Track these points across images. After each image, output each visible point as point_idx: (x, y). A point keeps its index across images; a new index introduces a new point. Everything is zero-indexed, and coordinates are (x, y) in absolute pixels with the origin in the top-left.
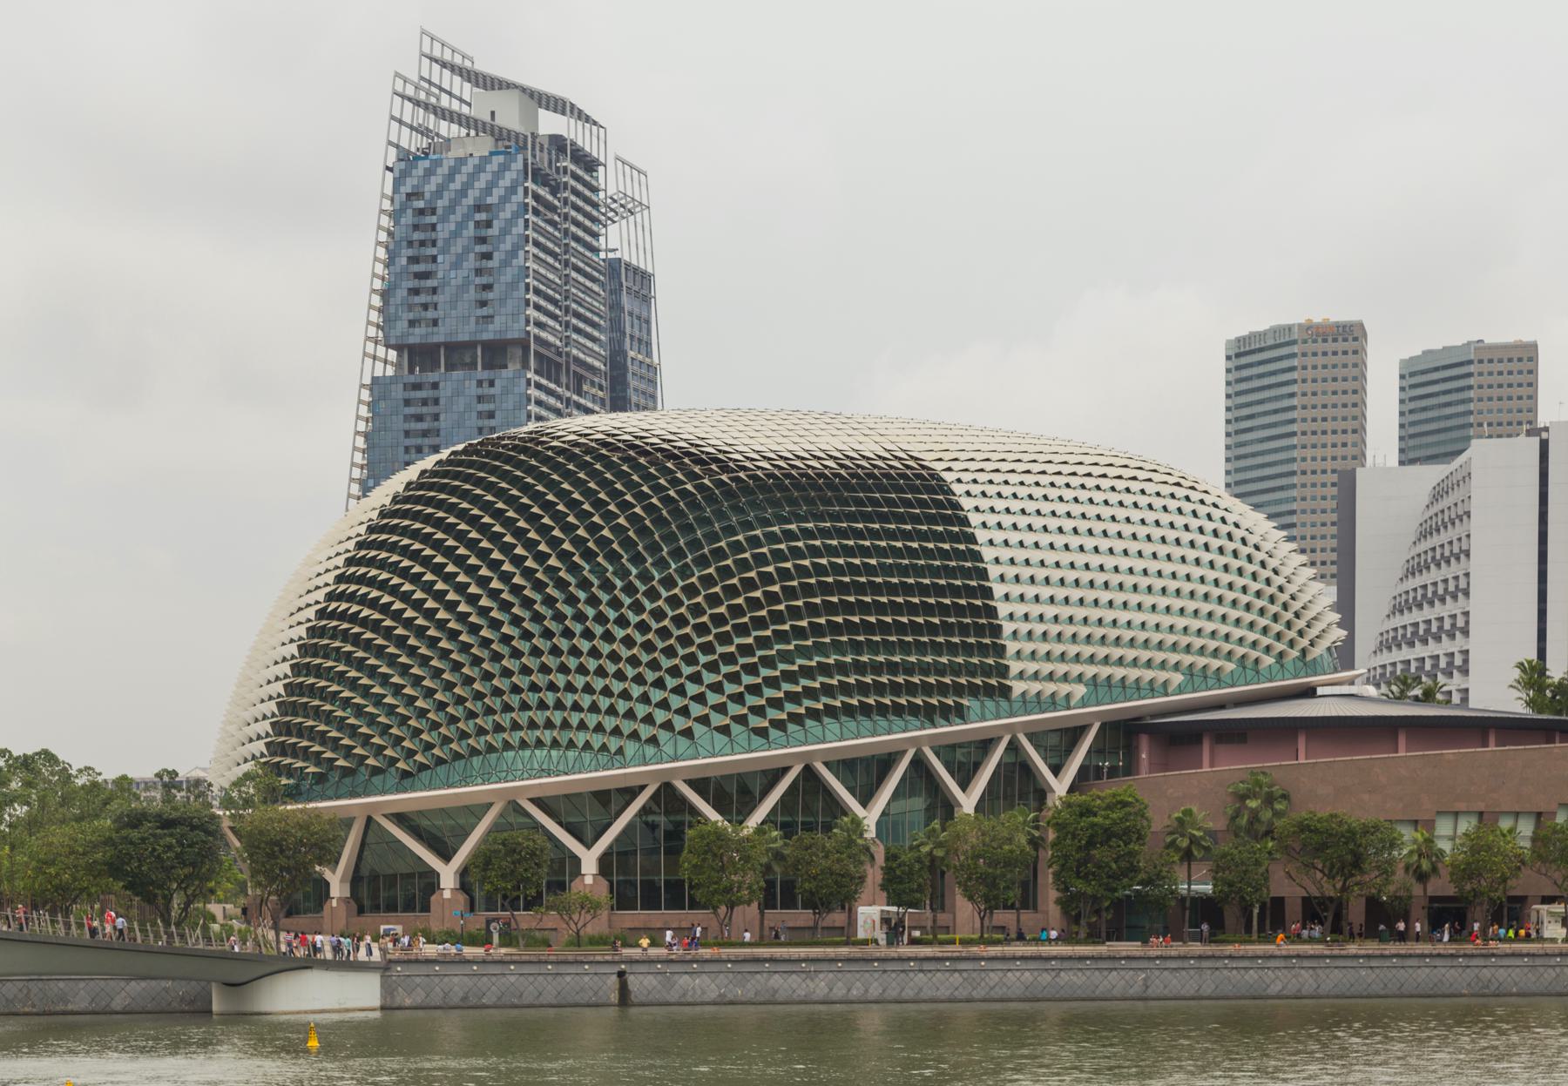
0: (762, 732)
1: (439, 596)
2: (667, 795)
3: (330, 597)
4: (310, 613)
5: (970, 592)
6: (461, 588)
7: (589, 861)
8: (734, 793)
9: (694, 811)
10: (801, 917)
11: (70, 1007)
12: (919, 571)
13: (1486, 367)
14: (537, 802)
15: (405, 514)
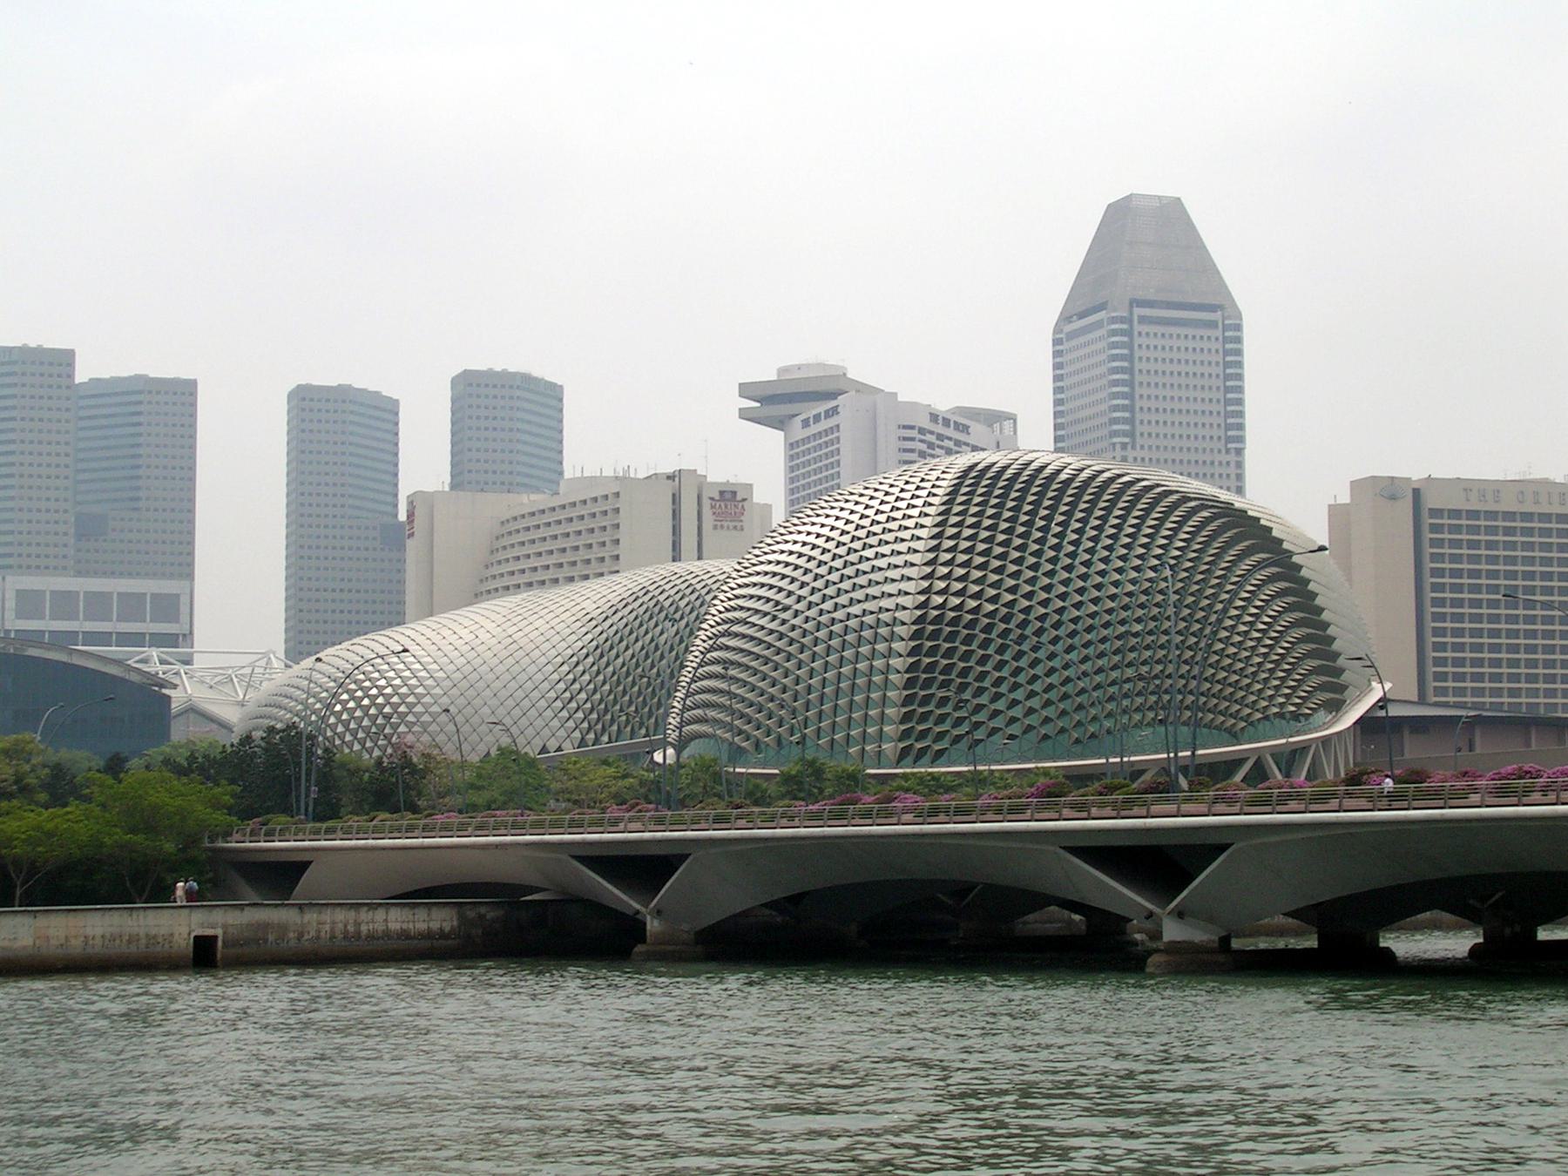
0: (1296, 717)
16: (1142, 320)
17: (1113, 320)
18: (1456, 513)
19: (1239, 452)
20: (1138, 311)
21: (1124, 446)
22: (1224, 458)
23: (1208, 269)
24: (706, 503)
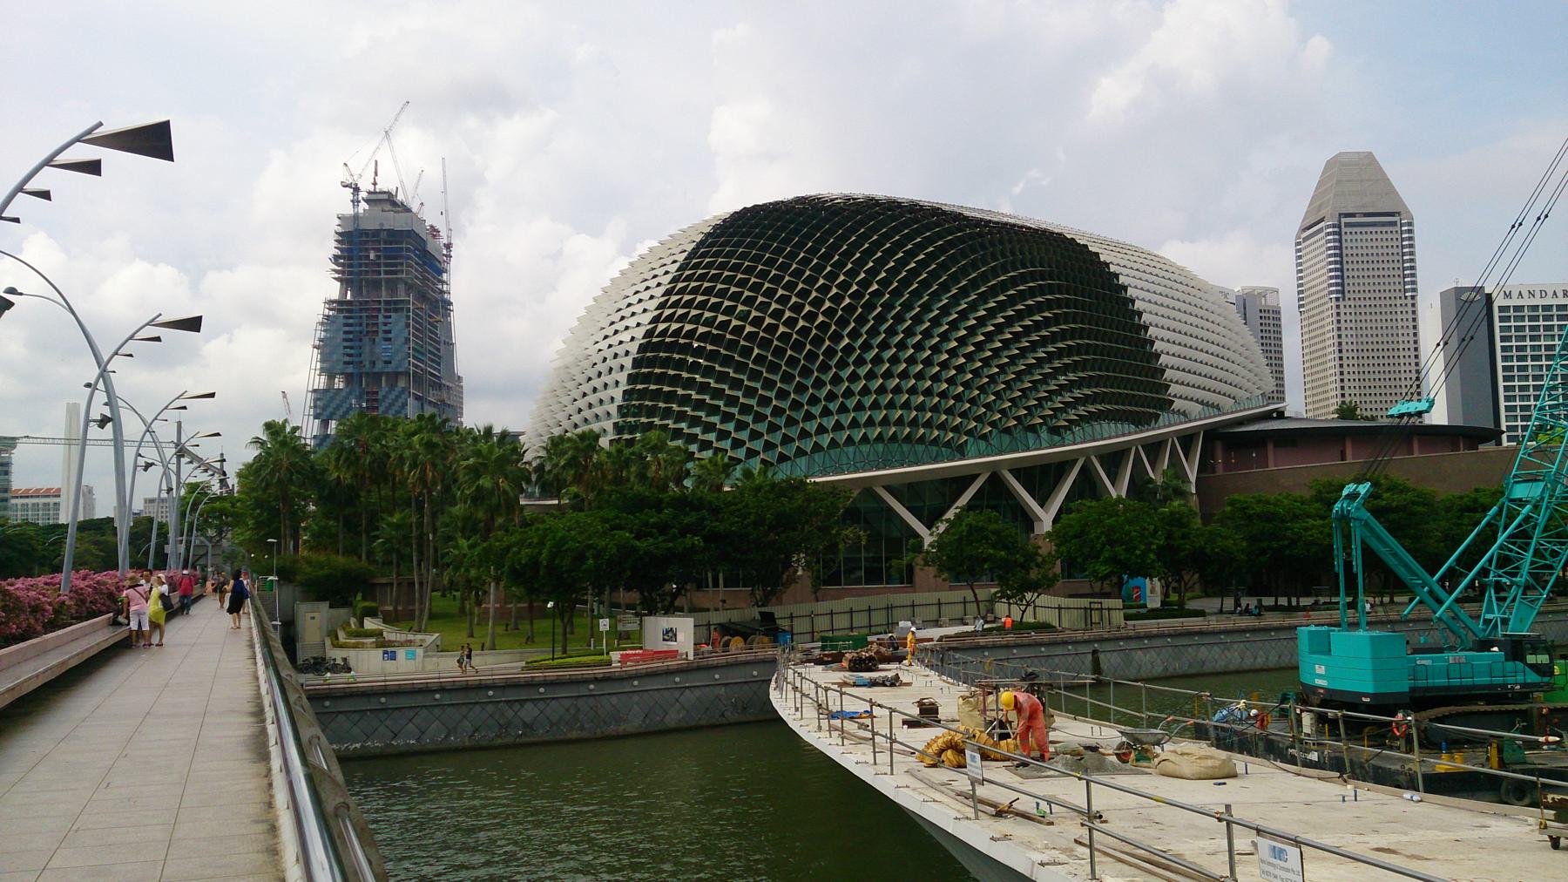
9: (1011, 494)
11: (623, 728)
14: (888, 489)
16: (1347, 225)
19: (1413, 297)
20: (1344, 220)
23: (1391, 191)
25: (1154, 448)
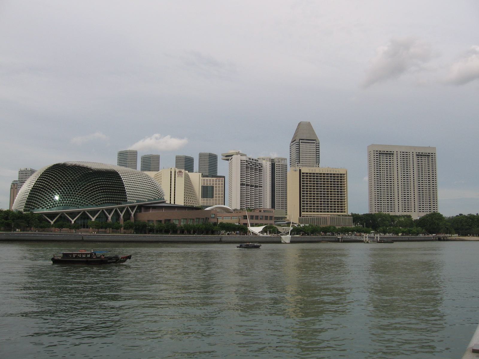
1: (47, 185)
2: (84, 213)
3: (35, 184)
4: (32, 186)
5: (122, 188)
6: (56, 184)
7: (73, 222)
8: (93, 213)
9: (87, 215)
10: (103, 230)
12: (116, 185)
13: (153, 158)
14: (66, 213)
15: (45, 173)
16: (301, 142)
17: (296, 142)
18: (307, 173)
19: (318, 164)
20: (300, 141)
21: (298, 163)
22: (316, 165)
23: (314, 134)
24: (176, 173)
25: (122, 209)
